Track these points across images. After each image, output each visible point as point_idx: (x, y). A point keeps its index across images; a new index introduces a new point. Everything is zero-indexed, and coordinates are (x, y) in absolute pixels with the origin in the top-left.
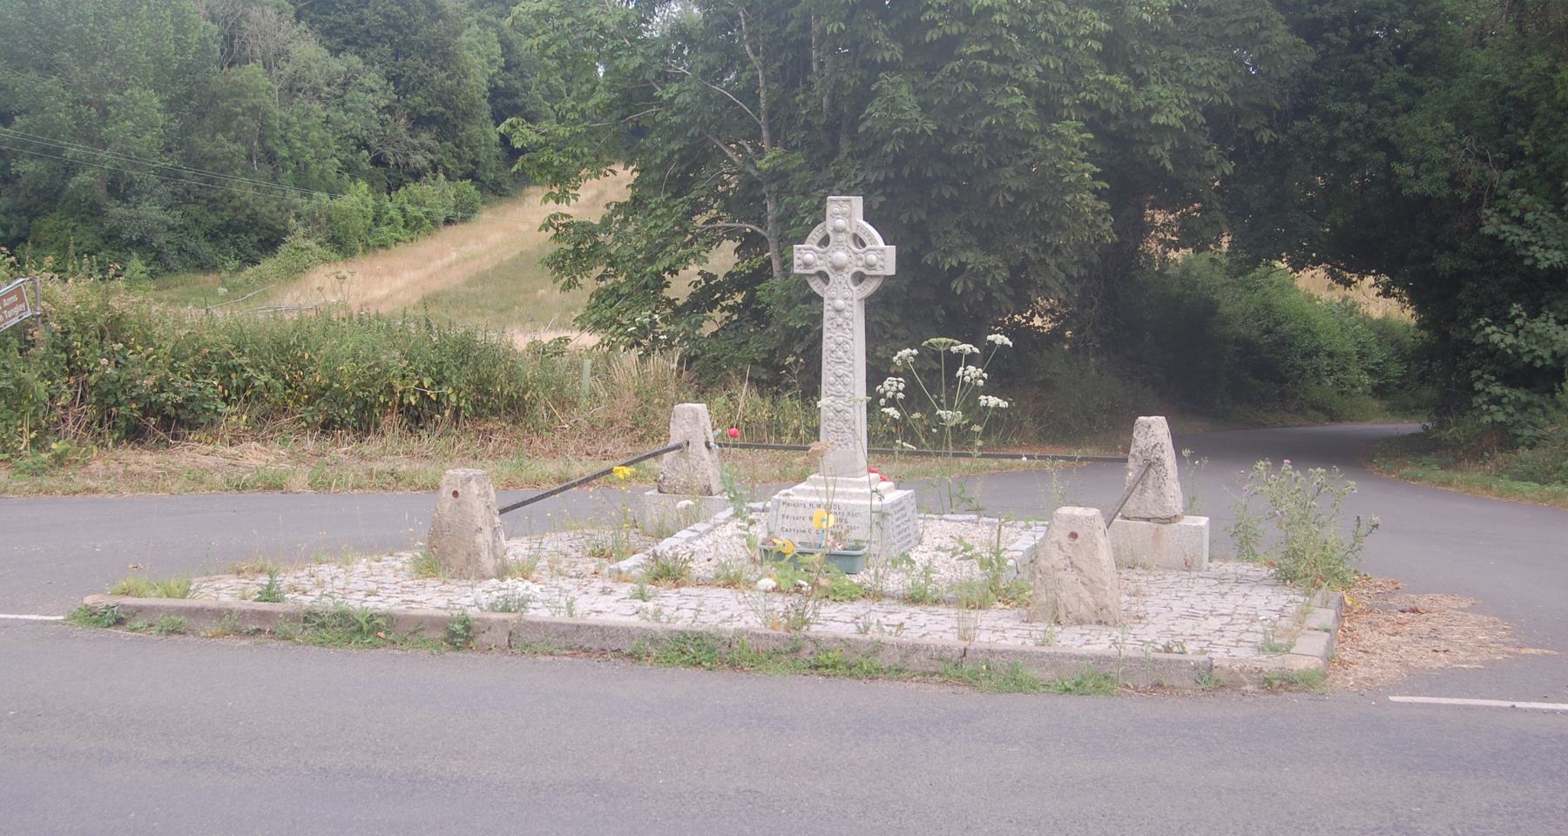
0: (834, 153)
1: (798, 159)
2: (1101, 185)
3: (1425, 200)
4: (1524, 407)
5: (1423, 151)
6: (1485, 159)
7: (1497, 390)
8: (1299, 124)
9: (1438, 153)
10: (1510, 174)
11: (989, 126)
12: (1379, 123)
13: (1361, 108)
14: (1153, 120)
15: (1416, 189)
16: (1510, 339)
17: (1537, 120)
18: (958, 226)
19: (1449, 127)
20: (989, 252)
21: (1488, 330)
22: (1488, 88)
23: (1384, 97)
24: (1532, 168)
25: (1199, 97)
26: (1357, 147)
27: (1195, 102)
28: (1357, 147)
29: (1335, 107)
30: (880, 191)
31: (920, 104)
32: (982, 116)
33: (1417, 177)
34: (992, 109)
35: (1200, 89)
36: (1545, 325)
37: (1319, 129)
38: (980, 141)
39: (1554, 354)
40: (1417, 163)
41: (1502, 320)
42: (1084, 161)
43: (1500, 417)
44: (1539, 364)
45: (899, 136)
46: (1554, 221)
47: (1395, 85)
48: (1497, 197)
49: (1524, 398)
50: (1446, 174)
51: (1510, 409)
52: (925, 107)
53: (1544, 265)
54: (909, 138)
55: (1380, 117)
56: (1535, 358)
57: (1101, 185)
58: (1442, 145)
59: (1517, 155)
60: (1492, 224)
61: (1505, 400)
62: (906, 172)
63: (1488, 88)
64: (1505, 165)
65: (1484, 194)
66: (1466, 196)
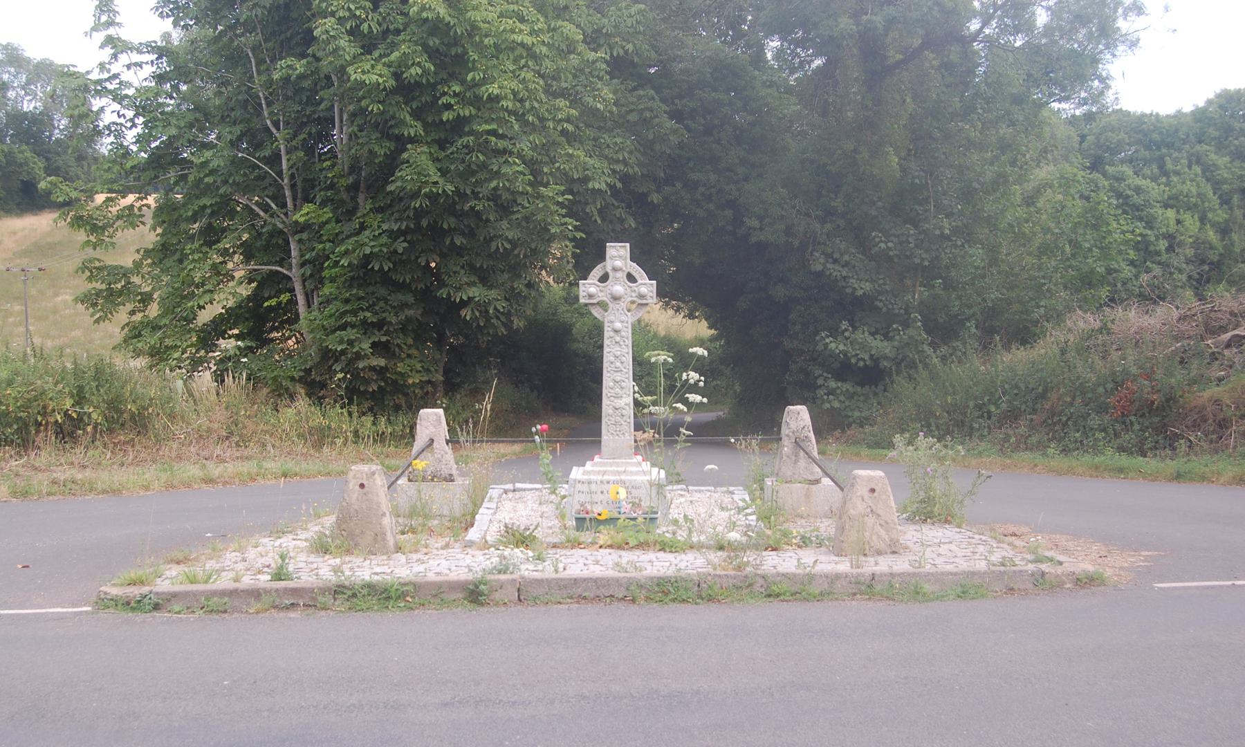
0: (355, 209)
1: (327, 214)
2: (579, 235)
3: (761, 247)
6: (808, 215)
7: (833, 384)
10: (828, 226)
11: (495, 189)
13: (713, 178)
14: (590, 186)
15: (762, 238)
16: (841, 347)
18: (463, 267)
20: (490, 287)
24: (841, 222)
25: (618, 167)
26: (711, 206)
27: (614, 171)
28: (711, 206)
29: (695, 176)
30: (402, 238)
31: (439, 170)
32: (490, 180)
33: (761, 229)
34: (497, 174)
35: (618, 161)
36: (862, 335)
38: (489, 200)
39: (872, 356)
41: (835, 332)
42: (564, 216)
43: (836, 404)
44: (861, 364)
45: (426, 195)
47: (737, 161)
49: (851, 390)
50: (783, 227)
51: (842, 398)
52: (444, 172)
53: (860, 293)
54: (433, 197)
57: (579, 235)
59: (830, 213)
62: (424, 223)
64: (823, 221)
66: (796, 243)
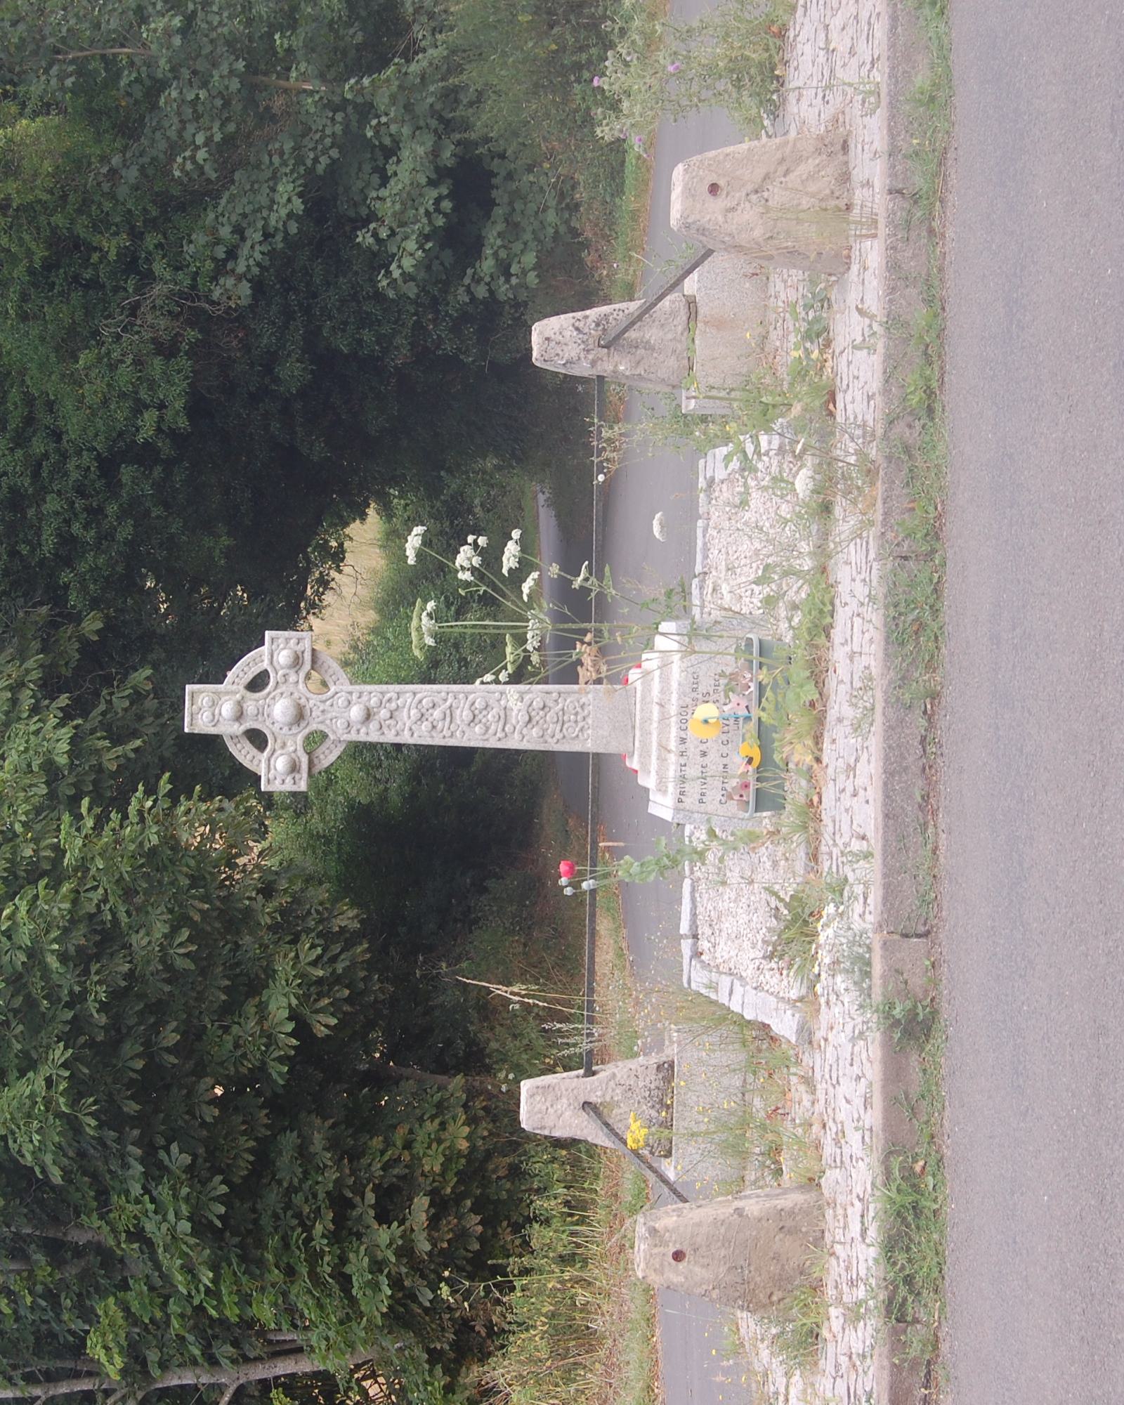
0: (99, 1249)
1: (108, 1308)
2: (164, 785)
3: (197, 407)
4: (513, 228)
5: (123, 395)
6: (134, 310)
7: (487, 266)
8: (73, 599)
9: (125, 373)
10: (159, 267)
11: (63, 958)
12: (75, 475)
13: (52, 504)
14: (62, 760)
15: (179, 404)
16: (411, 245)
17: (80, 231)
18: (226, 1029)
19: (85, 358)
20: (270, 973)
21: (396, 273)
22: (28, 307)
23: (36, 475)
24: (151, 240)
25: (26, 701)
26: (112, 509)
27: (35, 710)
28: (112, 509)
29: (49, 541)
30: (162, 1154)
31: (22, 1073)
32: (45, 969)
33: (162, 406)
34: (34, 953)
35: (14, 702)
36: (387, 201)
37: (83, 567)
38: (86, 972)
39: (432, 183)
40: (139, 408)
41: (380, 260)
42: (125, 816)
43: (530, 259)
44: (447, 205)
45: (73, 1103)
46: (232, 199)
47: (19, 453)
48: (194, 287)
49: (500, 227)
50: (158, 362)
51: (517, 247)
52: (28, 1065)
53: (298, 205)
54: (77, 1092)
55: (66, 474)
56: (438, 210)
57: (164, 785)
58: (113, 367)
59: (131, 263)
60: (235, 291)
61: (503, 254)
62: (132, 1107)
63: (28, 307)
64: (148, 278)
65: (190, 307)
66: (192, 334)
